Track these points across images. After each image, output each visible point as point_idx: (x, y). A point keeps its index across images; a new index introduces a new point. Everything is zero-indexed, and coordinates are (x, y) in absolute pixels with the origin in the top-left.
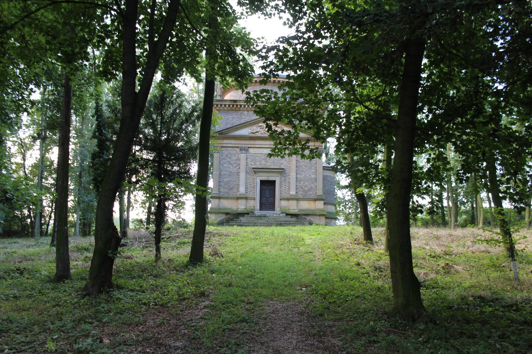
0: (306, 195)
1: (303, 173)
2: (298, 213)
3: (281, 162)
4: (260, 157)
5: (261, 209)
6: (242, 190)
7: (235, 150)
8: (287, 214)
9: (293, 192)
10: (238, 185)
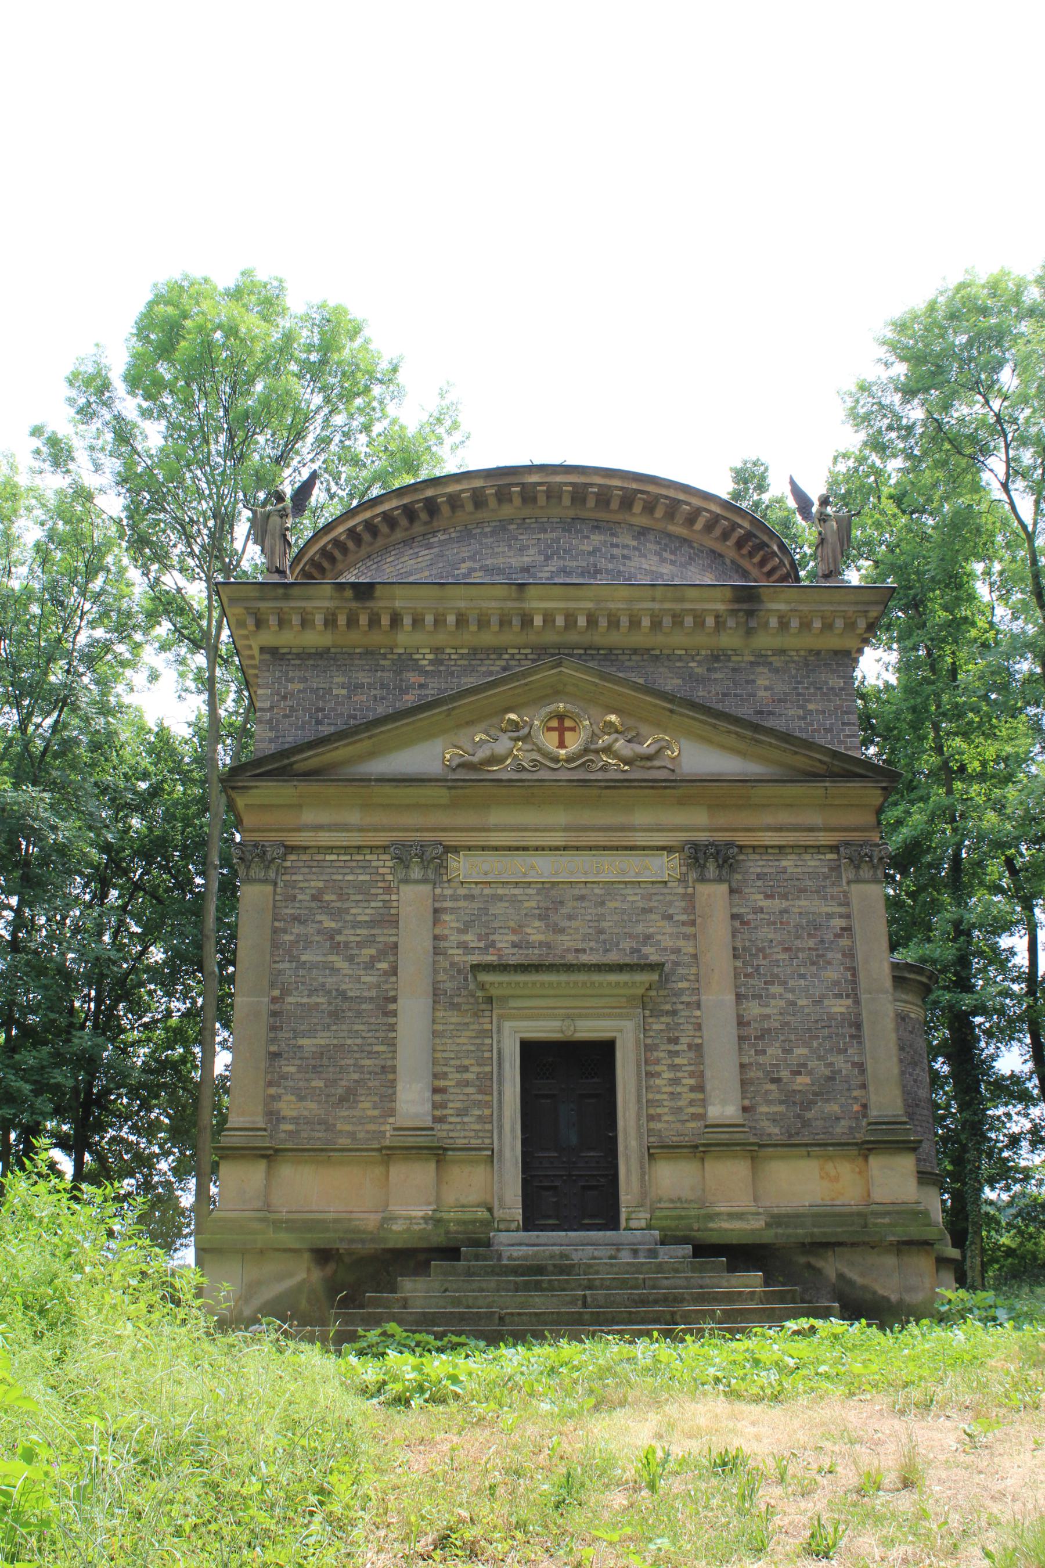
0: (806, 1123)
1: (776, 989)
2: (768, 1237)
3: (640, 929)
4: (514, 900)
5: (529, 1223)
6: (412, 1101)
7: (365, 867)
8: (703, 1250)
9: (723, 1109)
10: (388, 1071)
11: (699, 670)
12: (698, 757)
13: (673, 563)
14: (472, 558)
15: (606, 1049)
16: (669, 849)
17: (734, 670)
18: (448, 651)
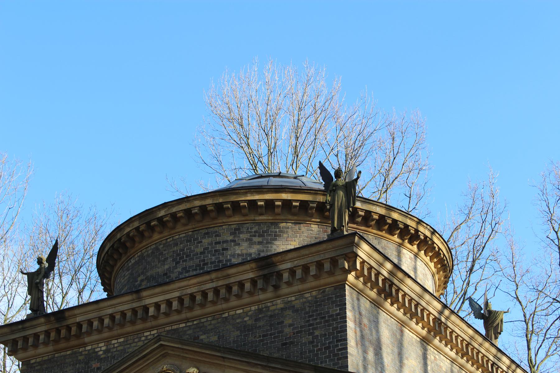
11: (250, 322)
13: (260, 243)
14: (143, 273)
17: (271, 316)
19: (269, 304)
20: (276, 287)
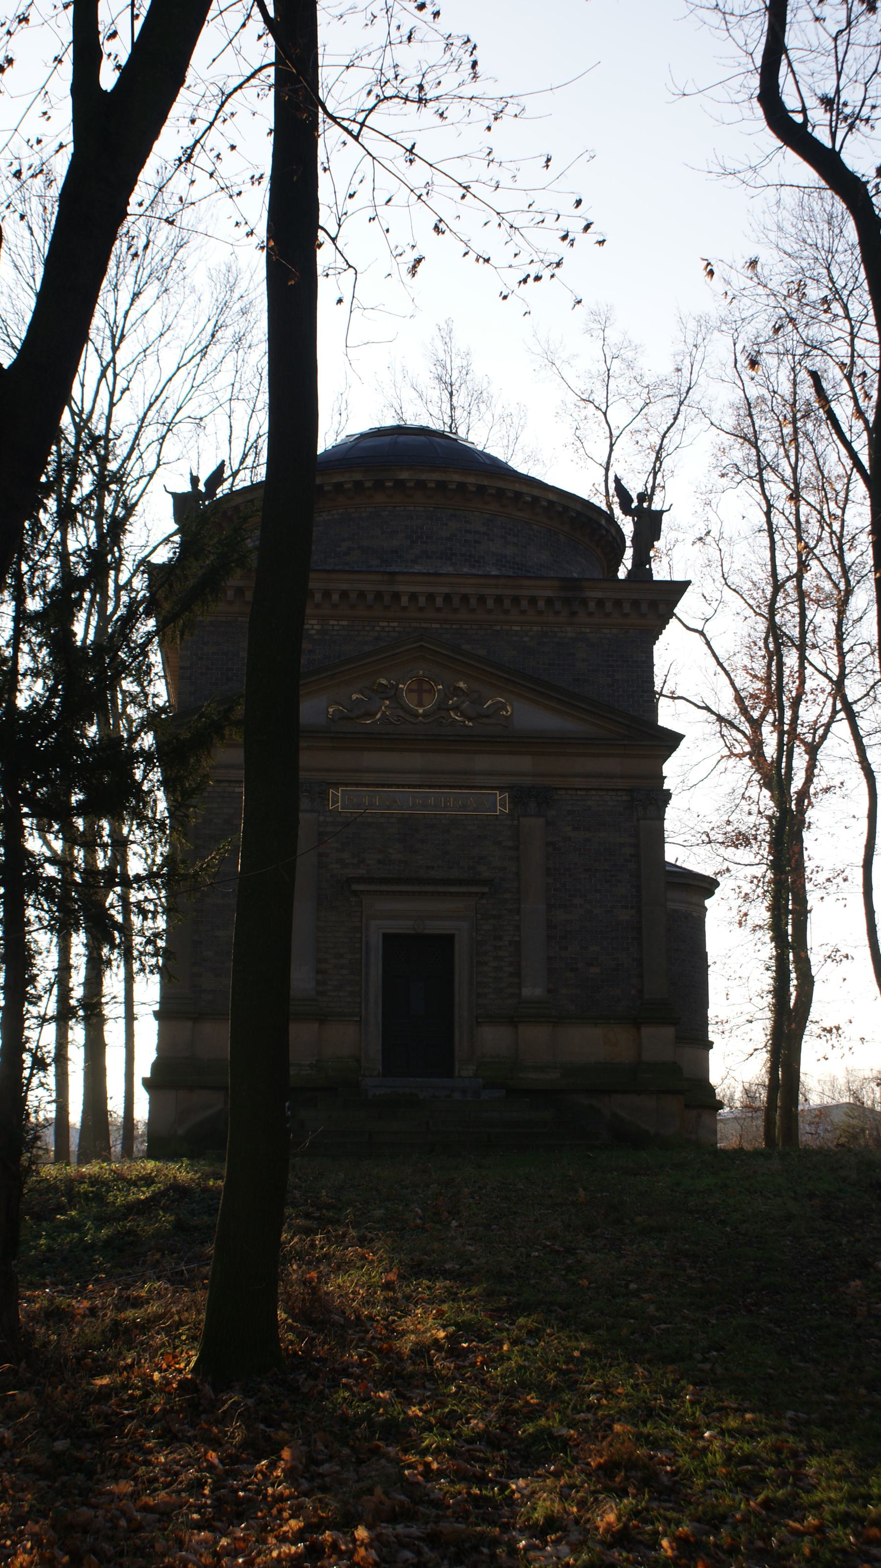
12: (528, 716)
15: (447, 941)
16: (501, 789)
18: (332, 622)
19: (556, 629)
20: (574, 614)
